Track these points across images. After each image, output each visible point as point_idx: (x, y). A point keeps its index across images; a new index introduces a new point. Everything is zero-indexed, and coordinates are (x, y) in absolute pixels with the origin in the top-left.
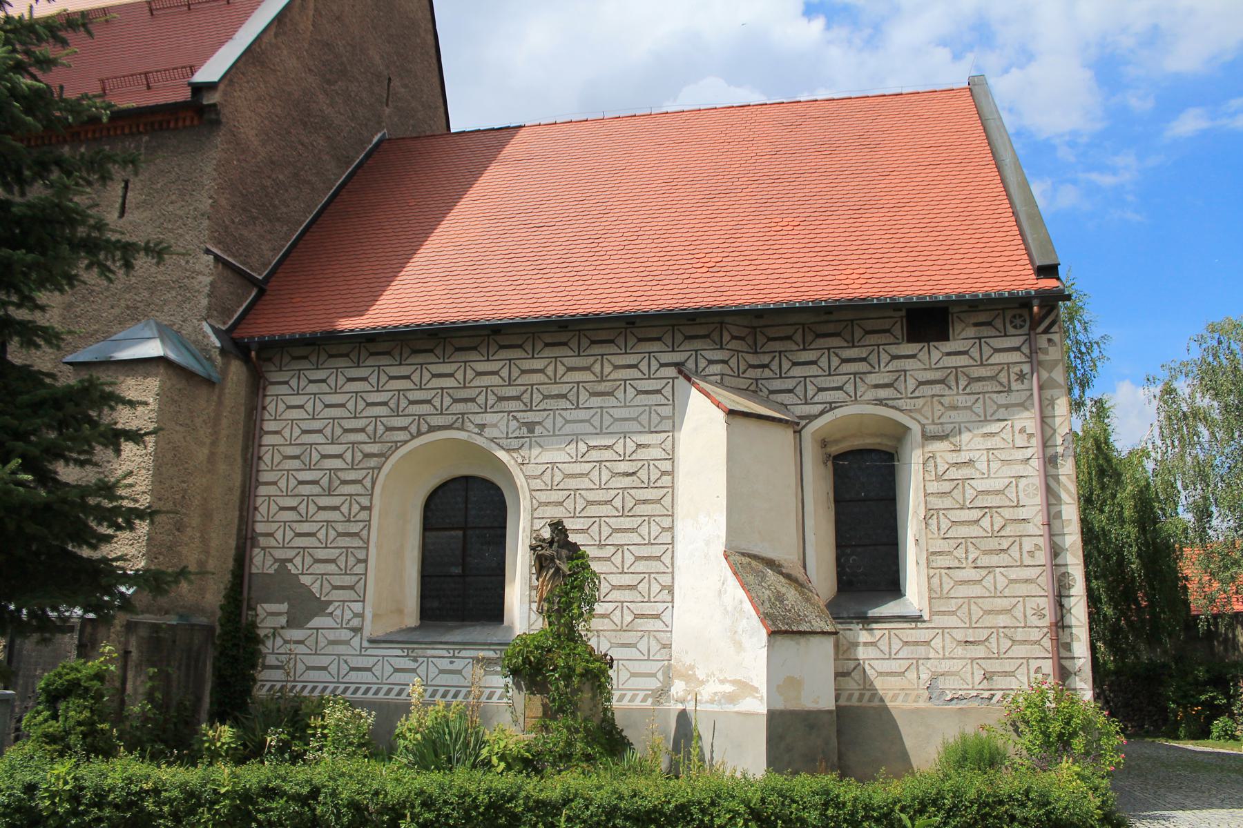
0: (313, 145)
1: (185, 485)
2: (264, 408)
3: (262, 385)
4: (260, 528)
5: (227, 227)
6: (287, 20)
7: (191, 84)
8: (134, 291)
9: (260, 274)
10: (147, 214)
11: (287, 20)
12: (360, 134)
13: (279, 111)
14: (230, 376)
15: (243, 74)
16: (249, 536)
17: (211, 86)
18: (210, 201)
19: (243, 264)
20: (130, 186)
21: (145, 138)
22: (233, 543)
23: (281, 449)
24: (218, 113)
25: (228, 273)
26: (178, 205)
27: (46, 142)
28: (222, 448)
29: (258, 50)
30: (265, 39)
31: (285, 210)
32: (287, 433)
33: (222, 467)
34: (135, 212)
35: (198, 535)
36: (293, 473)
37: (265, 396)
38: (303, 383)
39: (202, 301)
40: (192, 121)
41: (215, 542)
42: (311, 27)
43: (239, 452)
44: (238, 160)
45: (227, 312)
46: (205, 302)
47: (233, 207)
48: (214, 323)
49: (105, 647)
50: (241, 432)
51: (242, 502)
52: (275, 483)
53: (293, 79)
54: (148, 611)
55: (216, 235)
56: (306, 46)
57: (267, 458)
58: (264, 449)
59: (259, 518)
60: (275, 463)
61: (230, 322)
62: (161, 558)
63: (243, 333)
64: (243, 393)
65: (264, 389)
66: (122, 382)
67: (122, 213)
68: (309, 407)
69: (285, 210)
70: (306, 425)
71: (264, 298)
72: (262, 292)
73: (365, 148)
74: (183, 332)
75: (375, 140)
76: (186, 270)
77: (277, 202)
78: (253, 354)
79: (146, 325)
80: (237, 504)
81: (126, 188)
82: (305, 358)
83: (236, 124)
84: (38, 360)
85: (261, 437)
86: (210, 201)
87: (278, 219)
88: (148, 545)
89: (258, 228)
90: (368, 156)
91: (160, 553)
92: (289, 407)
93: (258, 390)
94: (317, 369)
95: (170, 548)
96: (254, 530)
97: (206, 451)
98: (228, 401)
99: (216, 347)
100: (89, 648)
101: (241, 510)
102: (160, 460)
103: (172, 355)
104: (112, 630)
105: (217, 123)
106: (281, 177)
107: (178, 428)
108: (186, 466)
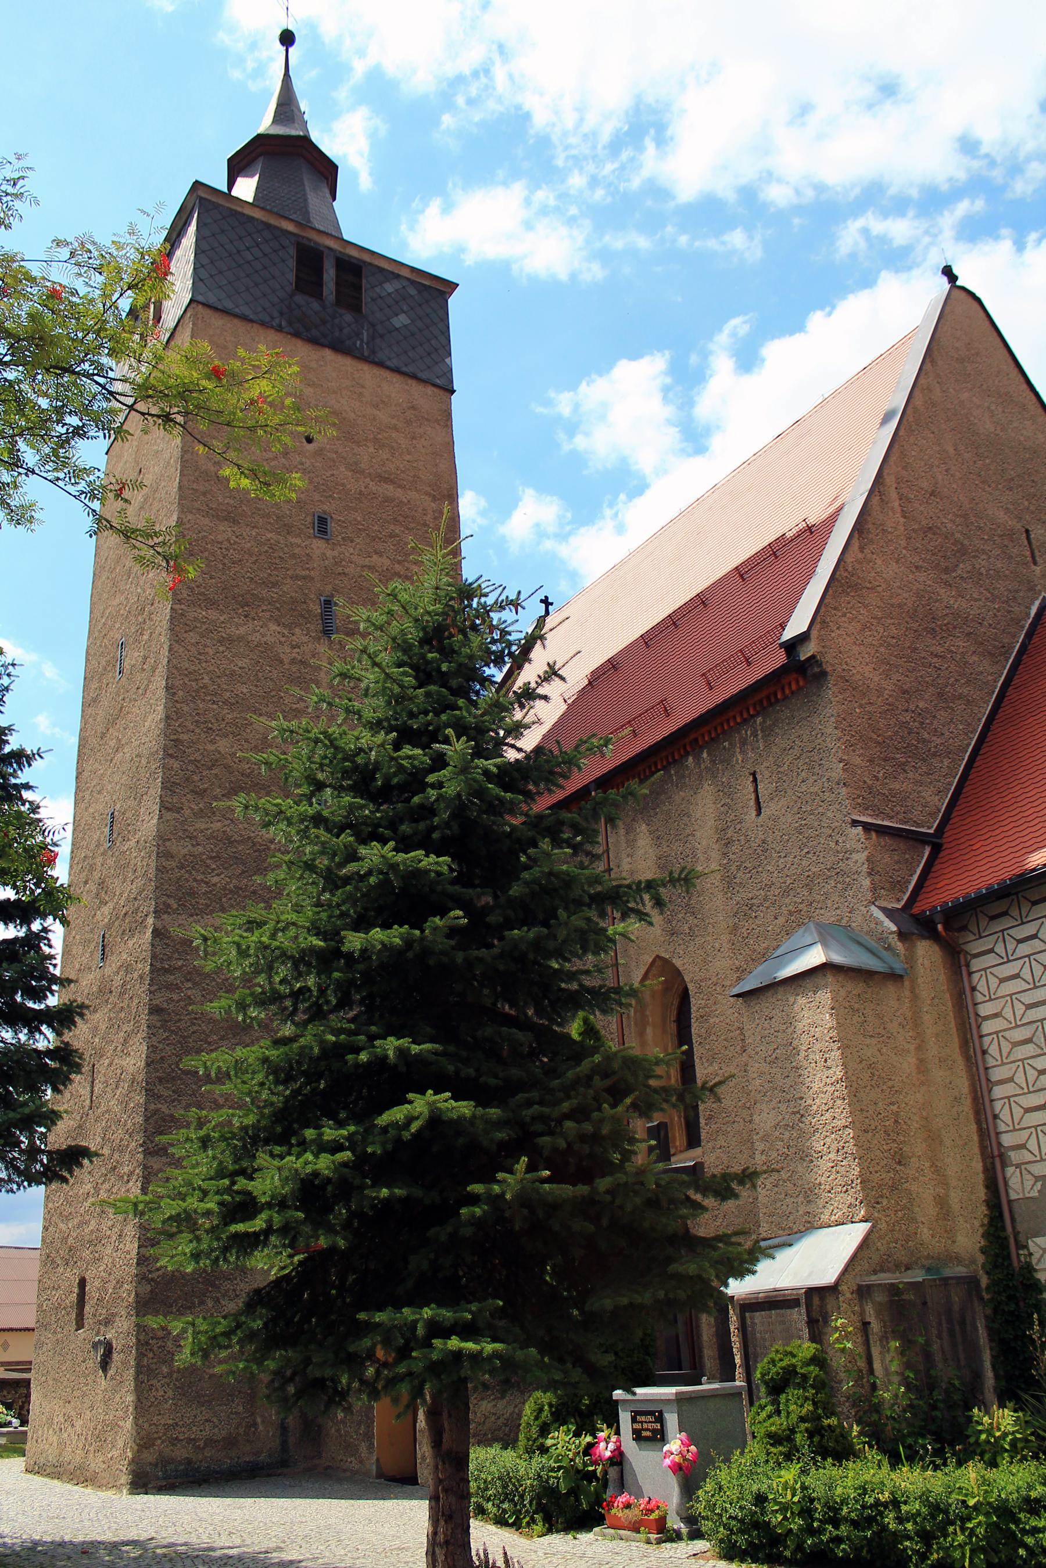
0: (951, 651)
1: (894, 1108)
2: (974, 989)
3: (963, 962)
4: (1007, 1140)
5: (869, 787)
6: (870, 526)
7: (782, 645)
8: (792, 893)
9: (929, 828)
10: (783, 802)
11: (870, 526)
12: (1009, 612)
13: (894, 631)
14: (920, 961)
15: (835, 609)
16: (996, 1153)
17: (802, 639)
18: (841, 765)
19: (905, 823)
20: (759, 777)
21: (759, 720)
22: (978, 1165)
23: (1007, 1034)
24: (820, 664)
25: (887, 840)
26: (811, 781)
27: (671, 760)
28: (933, 1050)
29: (846, 574)
30: (849, 559)
31: (939, 741)
32: (1008, 1013)
33: (938, 1075)
34: (770, 804)
35: (927, 1164)
36: (1029, 1061)
37: (970, 974)
38: (1011, 945)
39: (864, 883)
40: (797, 682)
41: (953, 1166)
42: (902, 520)
43: (957, 1050)
44: (861, 706)
45: (901, 885)
46: (867, 883)
47: (871, 761)
48: (884, 904)
49: (836, 1320)
50: (953, 1025)
51: (977, 1113)
52: (1011, 1080)
53: (900, 588)
54: (882, 1270)
55: (859, 801)
56: (903, 543)
57: (993, 1050)
58: (987, 1040)
59: (1002, 1127)
60: (1005, 1055)
61: (906, 898)
62: (885, 1202)
63: (923, 906)
64: (942, 978)
65: (968, 965)
66: (794, 1003)
67: (759, 813)
68: (1026, 974)
69: (939, 741)
70: (1028, 998)
71: (942, 854)
72: (937, 849)
73: (1023, 627)
74: (854, 924)
75: (1034, 611)
76: (838, 852)
77: (926, 736)
78: (940, 927)
79: (805, 932)
80: (971, 1116)
81: (755, 780)
82: (1005, 913)
83: (844, 667)
84: (719, 997)
85: (979, 1027)
86: (841, 765)
87: (934, 755)
88: (863, 1189)
89: (911, 775)
90: (1030, 635)
91: (882, 1197)
92: (1002, 980)
93: (960, 967)
94: (1023, 923)
95: (893, 1188)
96: (1000, 1144)
97: (913, 1060)
98: (925, 993)
99: (892, 933)
100: (821, 1323)
101: (978, 1122)
102: (855, 1085)
103: (837, 958)
104: (841, 1299)
105: (824, 674)
106: (921, 704)
107: (868, 1041)
108: (890, 1083)
